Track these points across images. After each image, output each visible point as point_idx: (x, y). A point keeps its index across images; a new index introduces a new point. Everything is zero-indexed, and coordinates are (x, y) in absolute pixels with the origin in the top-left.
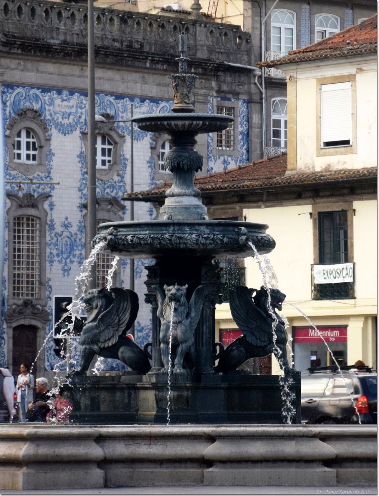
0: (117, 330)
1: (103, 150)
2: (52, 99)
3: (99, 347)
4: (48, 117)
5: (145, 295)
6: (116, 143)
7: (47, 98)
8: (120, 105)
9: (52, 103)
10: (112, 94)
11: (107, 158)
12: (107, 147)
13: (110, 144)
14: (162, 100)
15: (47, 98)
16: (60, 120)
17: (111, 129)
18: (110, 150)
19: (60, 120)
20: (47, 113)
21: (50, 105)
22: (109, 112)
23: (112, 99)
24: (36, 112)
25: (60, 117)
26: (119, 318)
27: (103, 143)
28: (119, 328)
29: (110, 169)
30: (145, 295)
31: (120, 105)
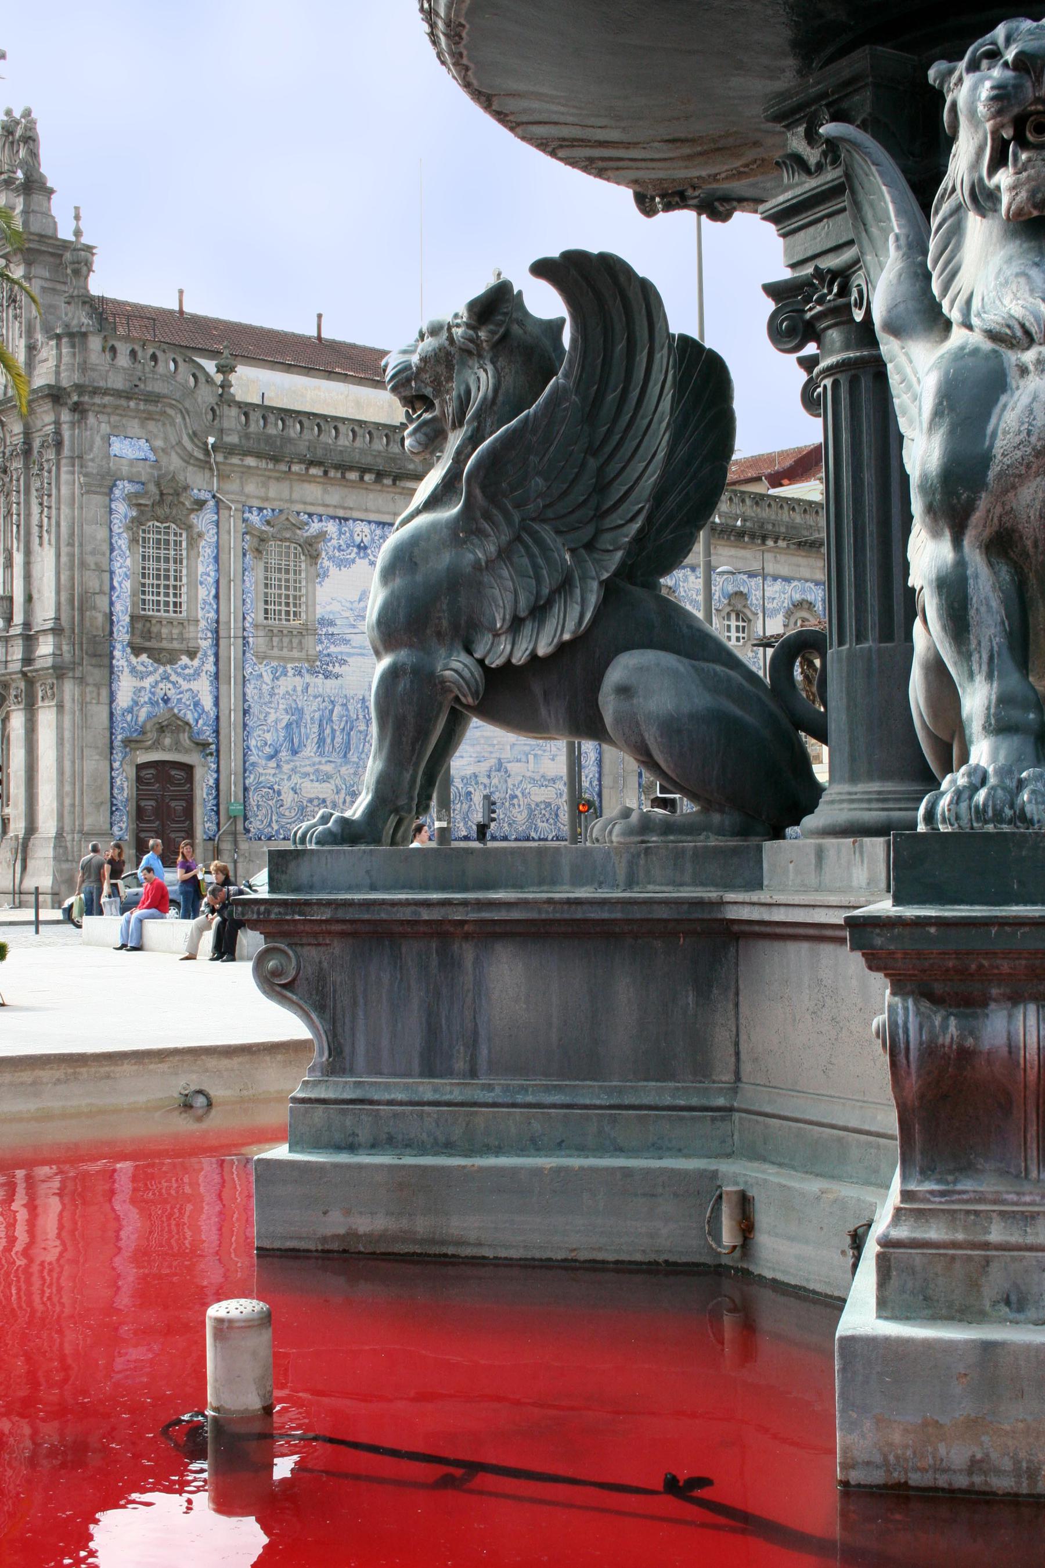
0: (590, 546)
1: (737, 627)
2: (686, 577)
3: (481, 662)
4: (683, 594)
5: (773, 290)
6: (750, 621)
7: (681, 575)
8: (753, 583)
9: (686, 580)
10: (745, 573)
11: (741, 635)
12: (741, 624)
13: (743, 621)
14: (794, 579)
15: (681, 575)
16: (694, 596)
17: (744, 606)
18: (744, 627)
19: (694, 596)
20: (682, 589)
21: (684, 582)
22: (742, 589)
23: (745, 577)
24: (670, 588)
25: (694, 594)
26: (601, 470)
27: (737, 620)
28: (598, 532)
29: (744, 645)
30: (773, 290)
31: (753, 583)
